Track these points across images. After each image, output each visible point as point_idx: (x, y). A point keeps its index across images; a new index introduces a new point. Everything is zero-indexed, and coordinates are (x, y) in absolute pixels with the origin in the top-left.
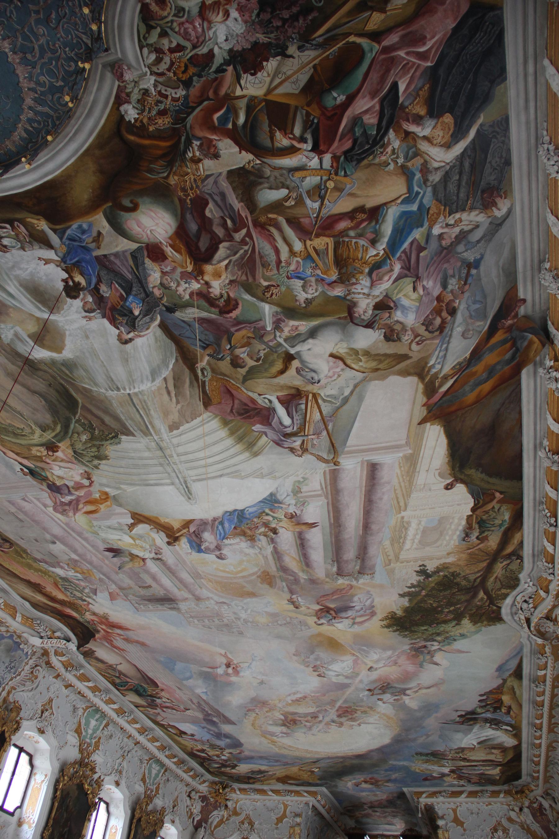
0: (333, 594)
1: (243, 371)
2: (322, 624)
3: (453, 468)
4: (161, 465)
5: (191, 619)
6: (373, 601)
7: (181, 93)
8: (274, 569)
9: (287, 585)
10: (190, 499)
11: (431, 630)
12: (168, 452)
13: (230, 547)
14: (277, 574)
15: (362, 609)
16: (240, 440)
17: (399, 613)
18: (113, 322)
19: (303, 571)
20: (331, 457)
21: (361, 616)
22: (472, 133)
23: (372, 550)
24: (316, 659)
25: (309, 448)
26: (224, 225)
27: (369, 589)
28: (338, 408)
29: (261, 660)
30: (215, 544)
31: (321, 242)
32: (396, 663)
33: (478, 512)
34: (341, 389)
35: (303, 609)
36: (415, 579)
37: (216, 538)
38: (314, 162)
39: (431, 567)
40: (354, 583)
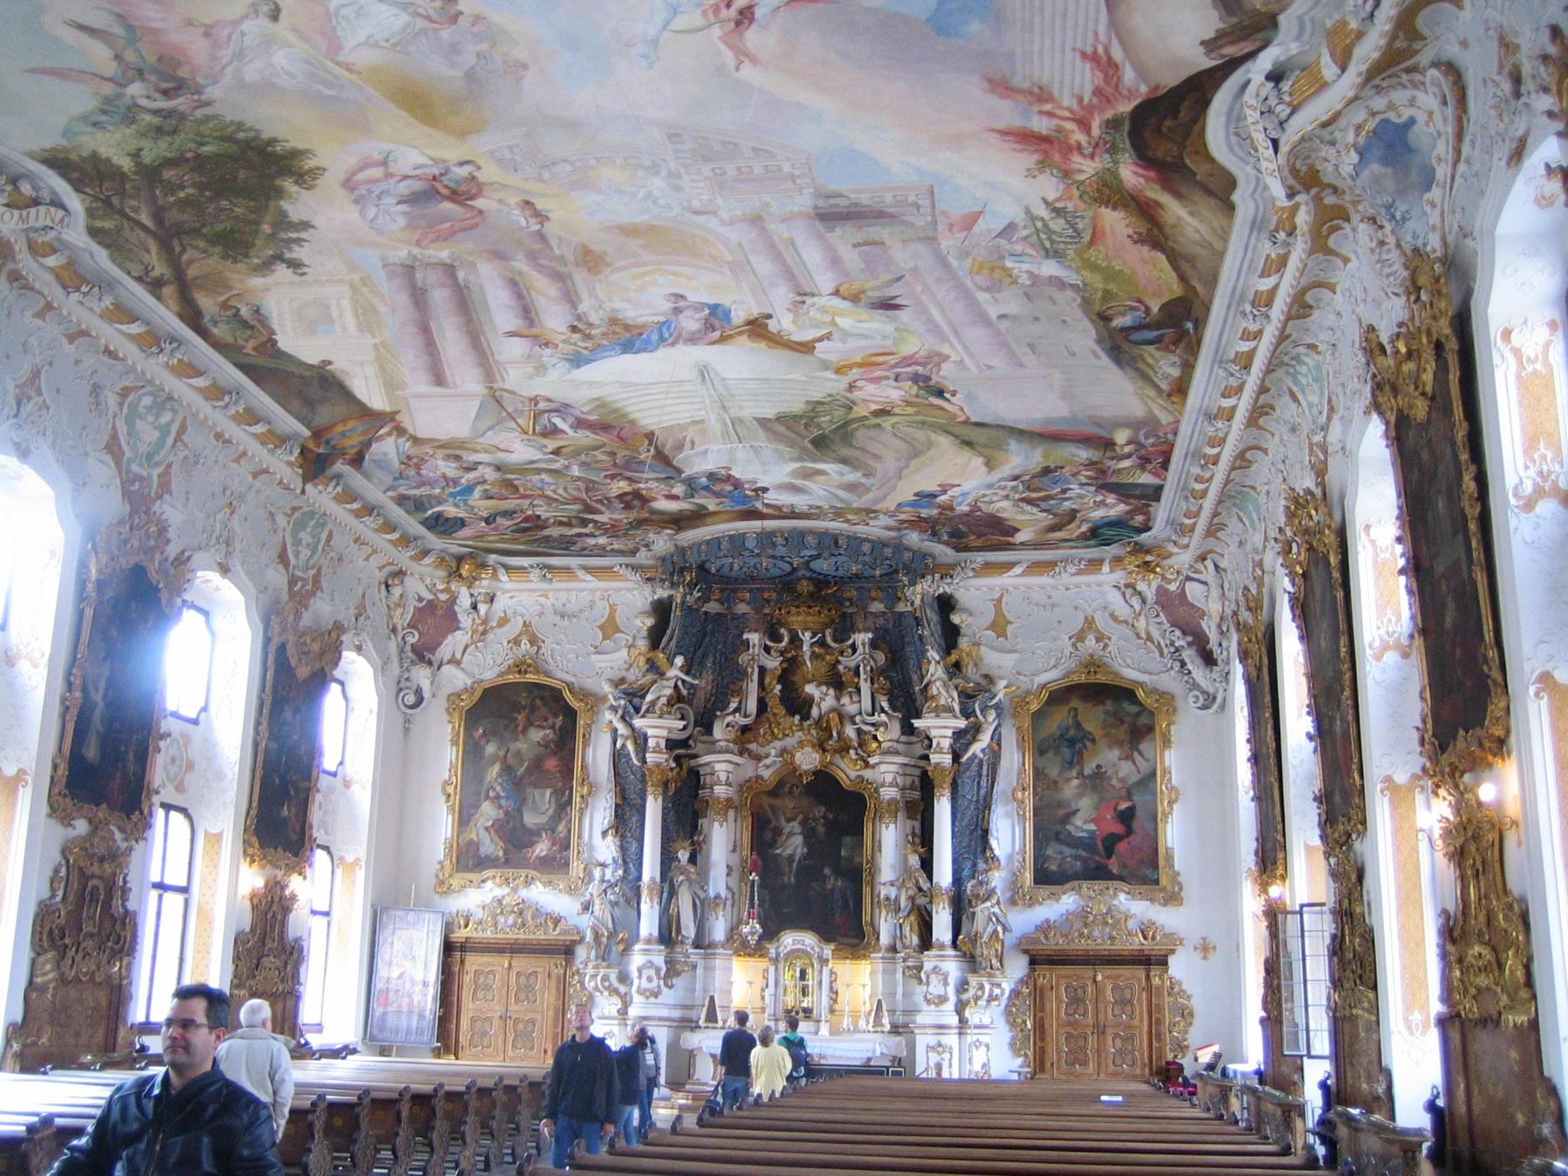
0: (452, 233)
2: (462, 164)
3: (334, 376)
4: (732, 395)
5: (797, 172)
6: (362, 213)
9: (552, 249)
11: (184, 142)
15: (379, 197)
16: (615, 410)
17: (289, 185)
18: (729, 477)
19: (520, 273)
21: (373, 181)
22: (430, 512)
23: (403, 300)
24: (454, 49)
27: (381, 240)
28: (498, 423)
29: (629, 45)
30: (681, 317)
31: (528, 492)
32: (207, 35)
33: (264, 339)
35: (514, 200)
36: (299, 253)
39: (282, 272)
40: (415, 251)
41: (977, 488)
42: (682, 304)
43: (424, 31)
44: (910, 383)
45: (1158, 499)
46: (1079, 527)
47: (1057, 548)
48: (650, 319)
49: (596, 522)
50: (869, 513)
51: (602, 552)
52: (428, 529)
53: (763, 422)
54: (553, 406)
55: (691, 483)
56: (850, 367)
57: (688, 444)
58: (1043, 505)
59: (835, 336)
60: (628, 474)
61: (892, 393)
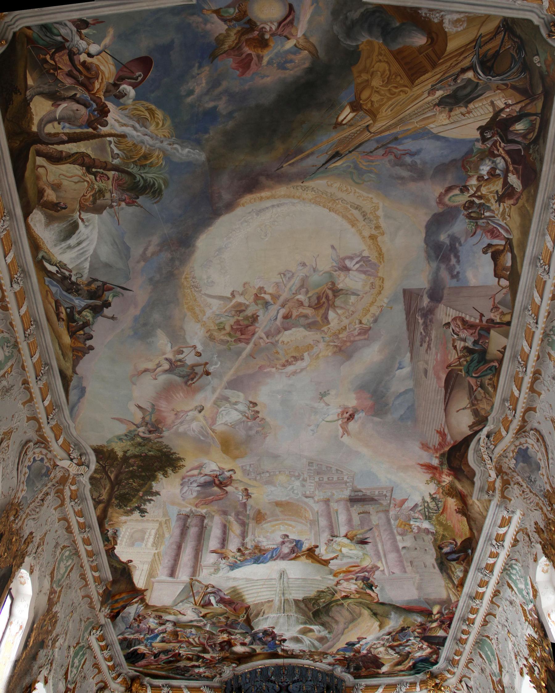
1: (225, 615)
4: (289, 587)
7: (217, 665)
8: (251, 525)
10: (283, 572)
12: (282, 592)
13: (275, 543)
14: (251, 521)
16: (238, 594)
18: (273, 632)
20: (194, 582)
22: (132, 649)
24: (250, 428)
25: (204, 587)
26: (215, 646)
28: (186, 599)
30: (284, 545)
34: (183, 605)
37: (281, 549)
38: (180, 652)
41: (371, 640)
42: (286, 540)
43: (244, 422)
44: (361, 581)
45: (443, 645)
46: (409, 663)
47: (397, 676)
48: (271, 546)
49: (203, 658)
50: (324, 654)
51: (199, 677)
52: (126, 659)
53: (296, 602)
54: (214, 590)
55: (255, 637)
56: (340, 573)
57: (262, 613)
58: (397, 650)
59: (339, 558)
60: (230, 630)
61: (351, 587)
